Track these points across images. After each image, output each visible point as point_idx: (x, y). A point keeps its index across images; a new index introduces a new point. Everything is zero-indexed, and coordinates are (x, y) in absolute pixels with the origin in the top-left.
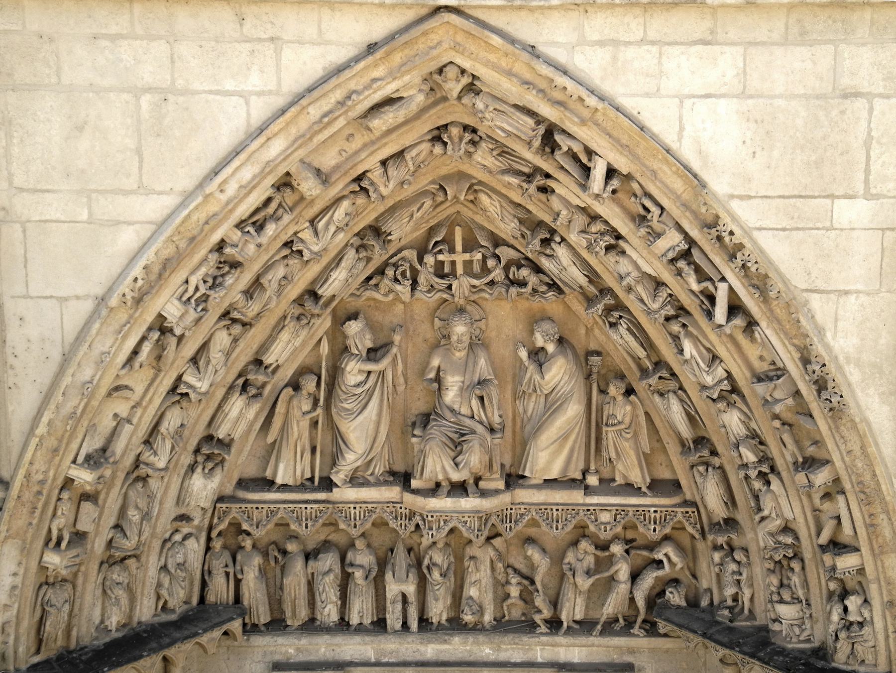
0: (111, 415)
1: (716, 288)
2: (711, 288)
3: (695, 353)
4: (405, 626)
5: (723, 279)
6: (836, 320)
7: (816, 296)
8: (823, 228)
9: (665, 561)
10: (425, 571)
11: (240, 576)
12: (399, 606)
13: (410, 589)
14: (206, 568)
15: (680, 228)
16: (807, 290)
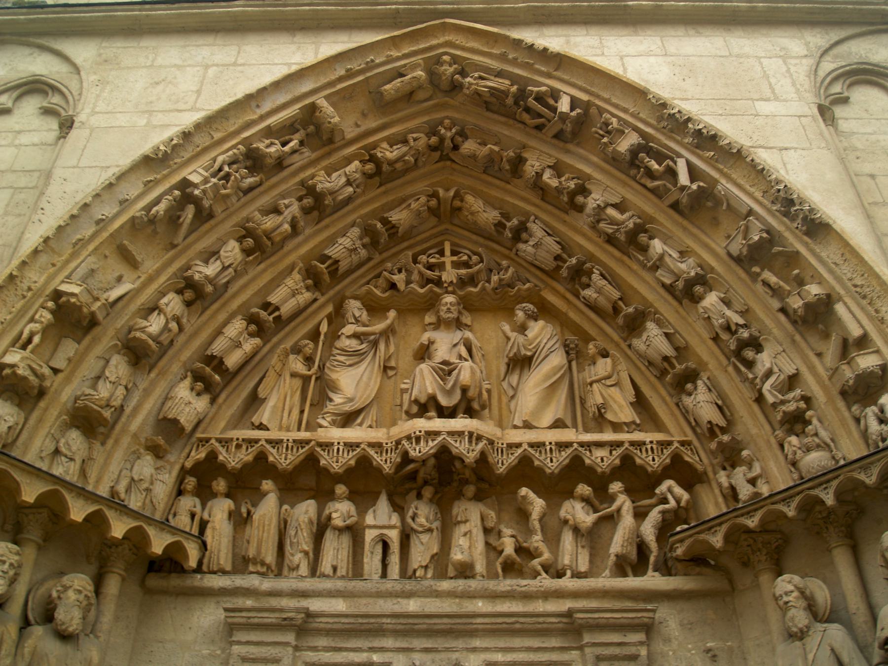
0: (117, 274)
1: (675, 163)
2: (671, 163)
3: (666, 248)
4: (384, 575)
5: (680, 156)
6: (784, 164)
7: (760, 150)
8: (752, 115)
9: (670, 497)
10: (409, 520)
11: (206, 516)
12: (378, 556)
13: (394, 535)
14: (172, 512)
15: (636, 129)
16: (752, 147)
